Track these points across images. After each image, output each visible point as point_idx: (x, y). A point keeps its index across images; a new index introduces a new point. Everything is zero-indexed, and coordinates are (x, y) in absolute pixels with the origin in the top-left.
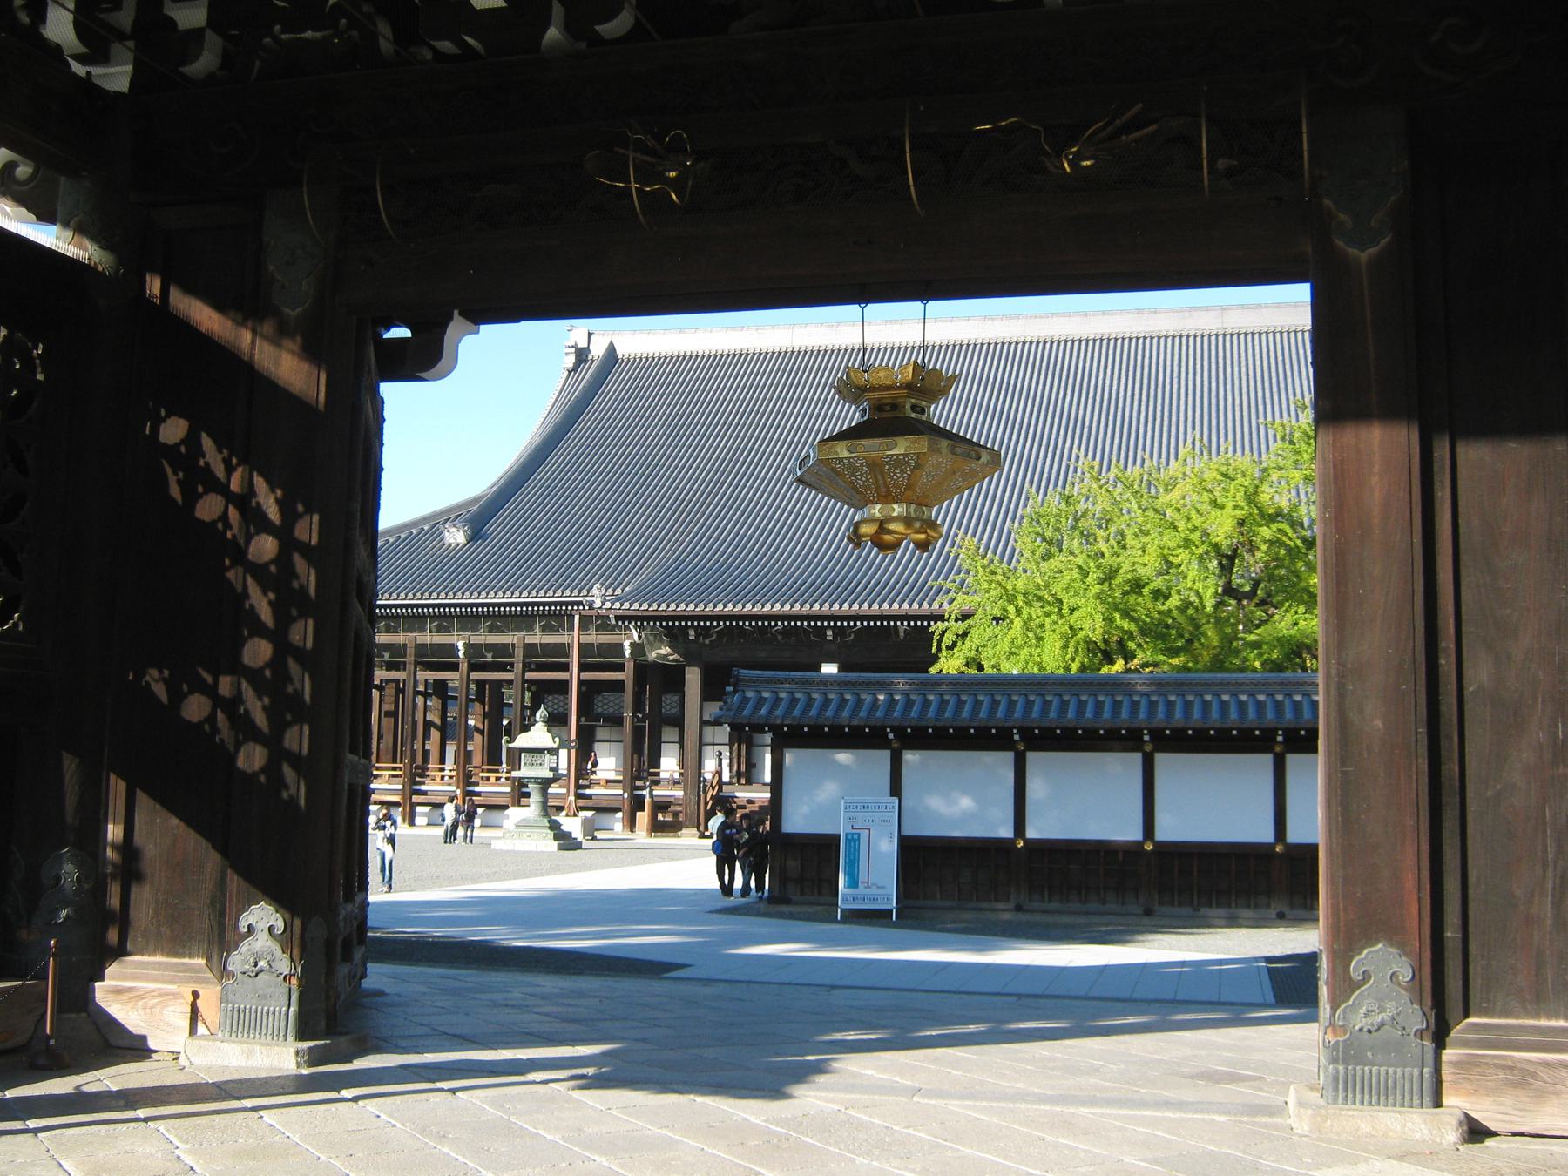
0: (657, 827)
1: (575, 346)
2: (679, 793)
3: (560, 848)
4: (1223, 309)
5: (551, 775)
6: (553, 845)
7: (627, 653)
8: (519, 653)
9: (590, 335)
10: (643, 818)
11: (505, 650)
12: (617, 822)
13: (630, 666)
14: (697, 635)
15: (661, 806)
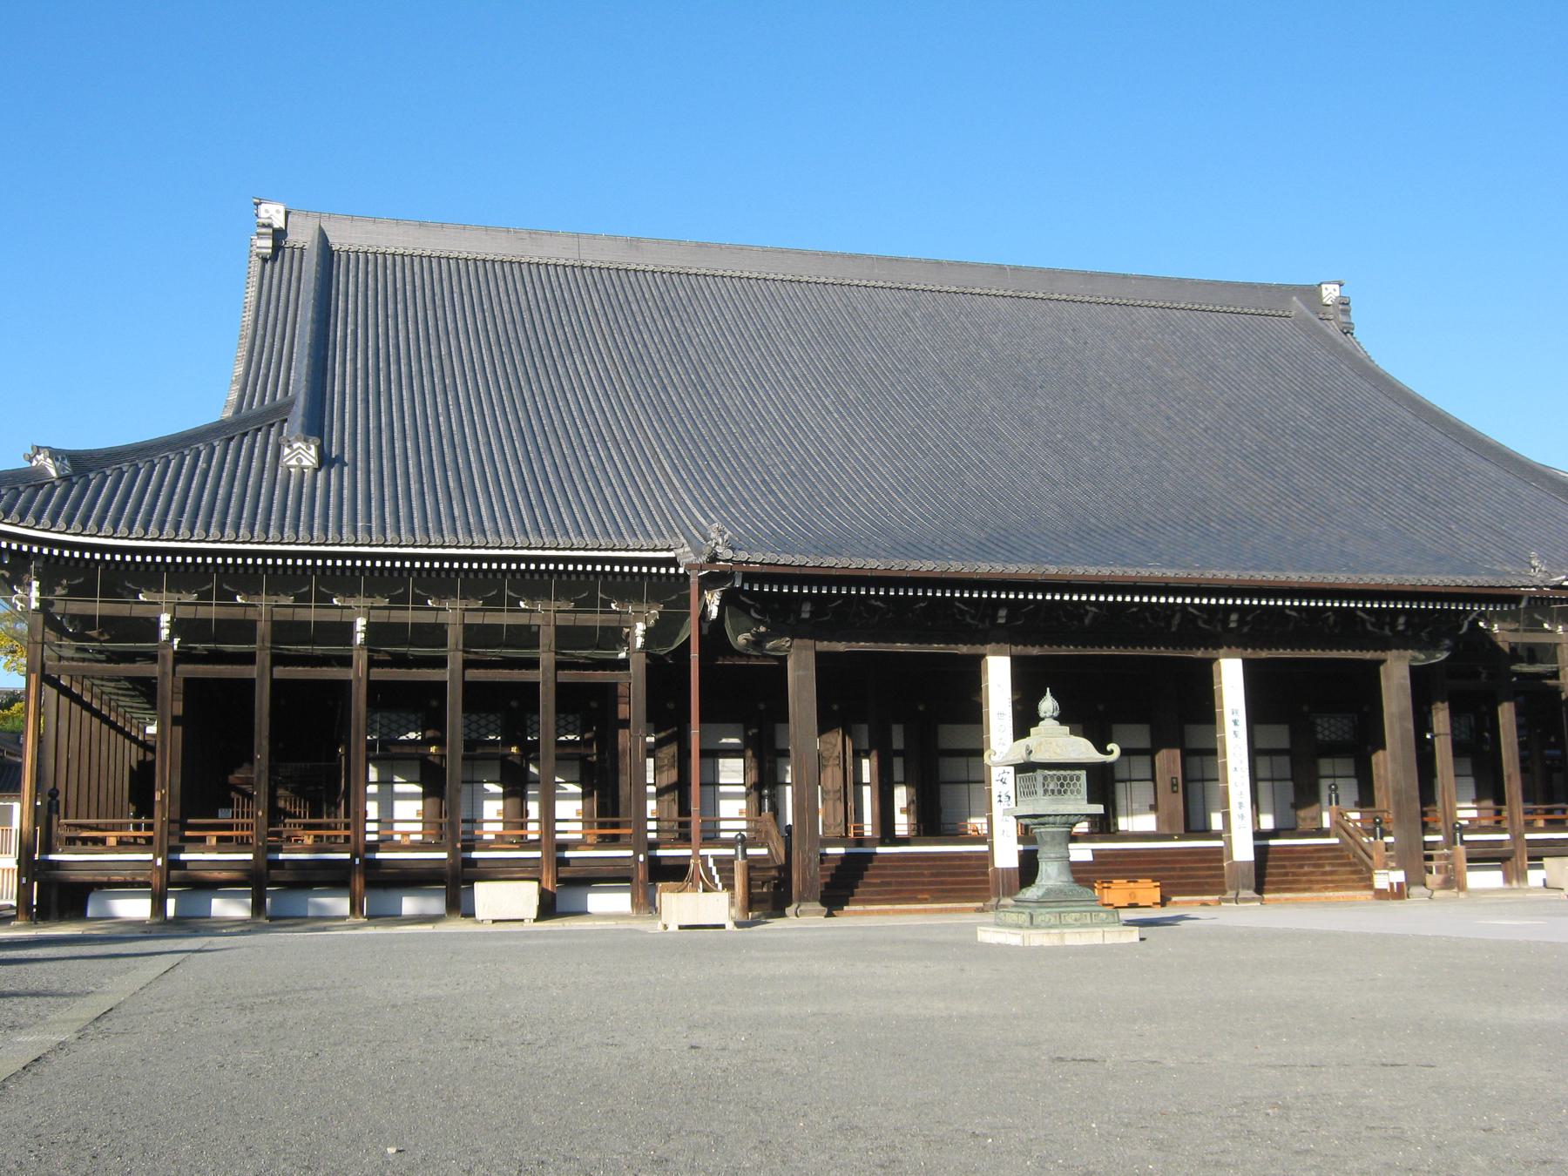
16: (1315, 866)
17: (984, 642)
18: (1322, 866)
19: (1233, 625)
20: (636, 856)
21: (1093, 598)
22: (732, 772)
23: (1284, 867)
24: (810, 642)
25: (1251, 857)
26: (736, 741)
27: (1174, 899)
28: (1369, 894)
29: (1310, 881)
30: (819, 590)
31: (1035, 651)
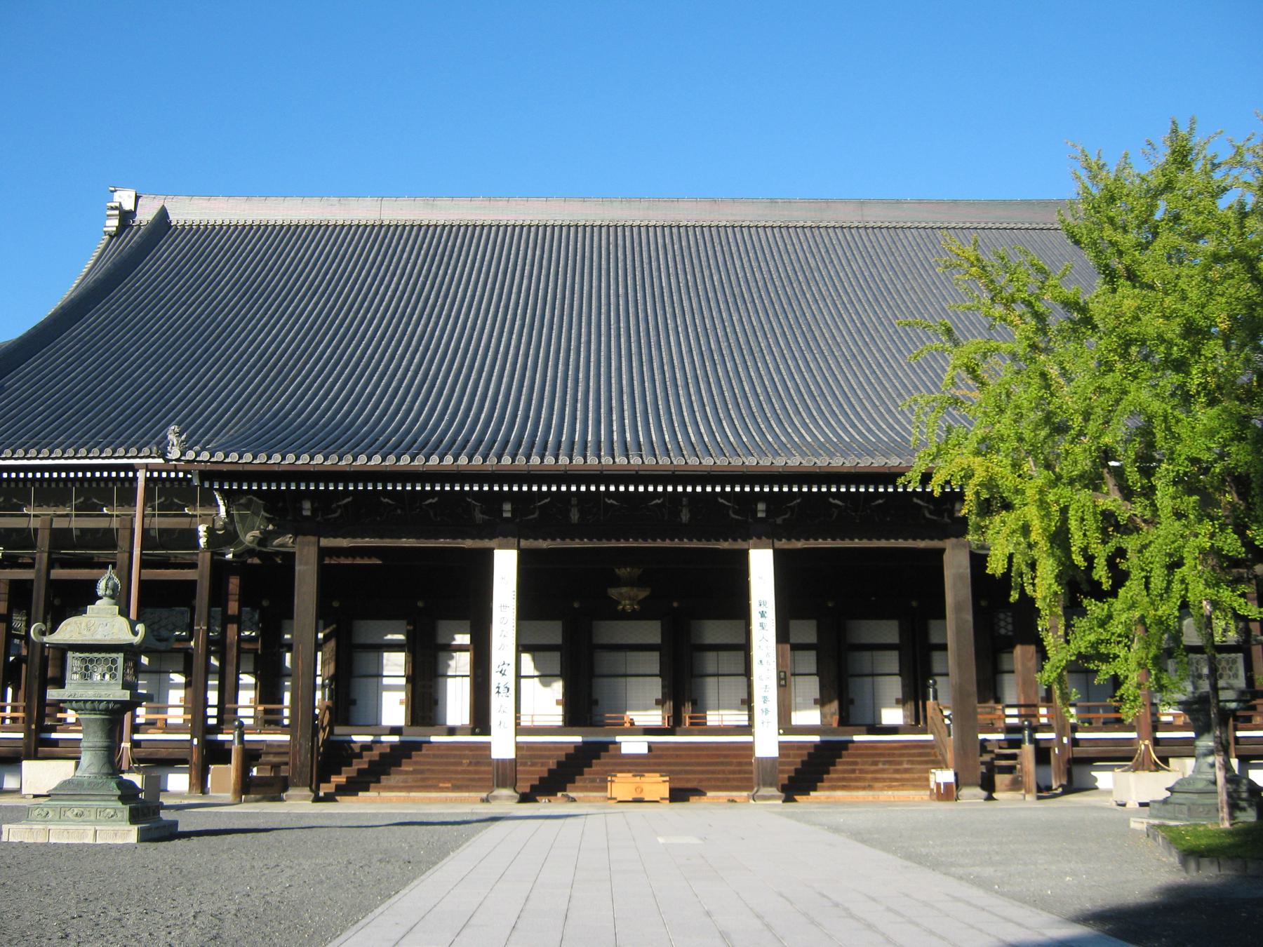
0: (247, 787)
1: (120, 208)
2: (287, 738)
3: (144, 837)
4: (862, 203)
5: (126, 695)
6: (131, 834)
7: (202, 541)
8: (43, 541)
9: (137, 198)
10: (224, 776)
11: (24, 538)
12: (178, 782)
13: (204, 559)
14: (314, 510)
15: (251, 755)
16: (890, 763)
17: (491, 536)
18: (900, 763)
19: (760, 515)
20: (191, 741)
21: (612, 488)
22: (395, 664)
23: (855, 763)
24: (313, 539)
25: (774, 752)
26: (401, 637)
27: (710, 794)
28: (925, 794)
29: (876, 780)
30: (317, 486)
31: (544, 544)
